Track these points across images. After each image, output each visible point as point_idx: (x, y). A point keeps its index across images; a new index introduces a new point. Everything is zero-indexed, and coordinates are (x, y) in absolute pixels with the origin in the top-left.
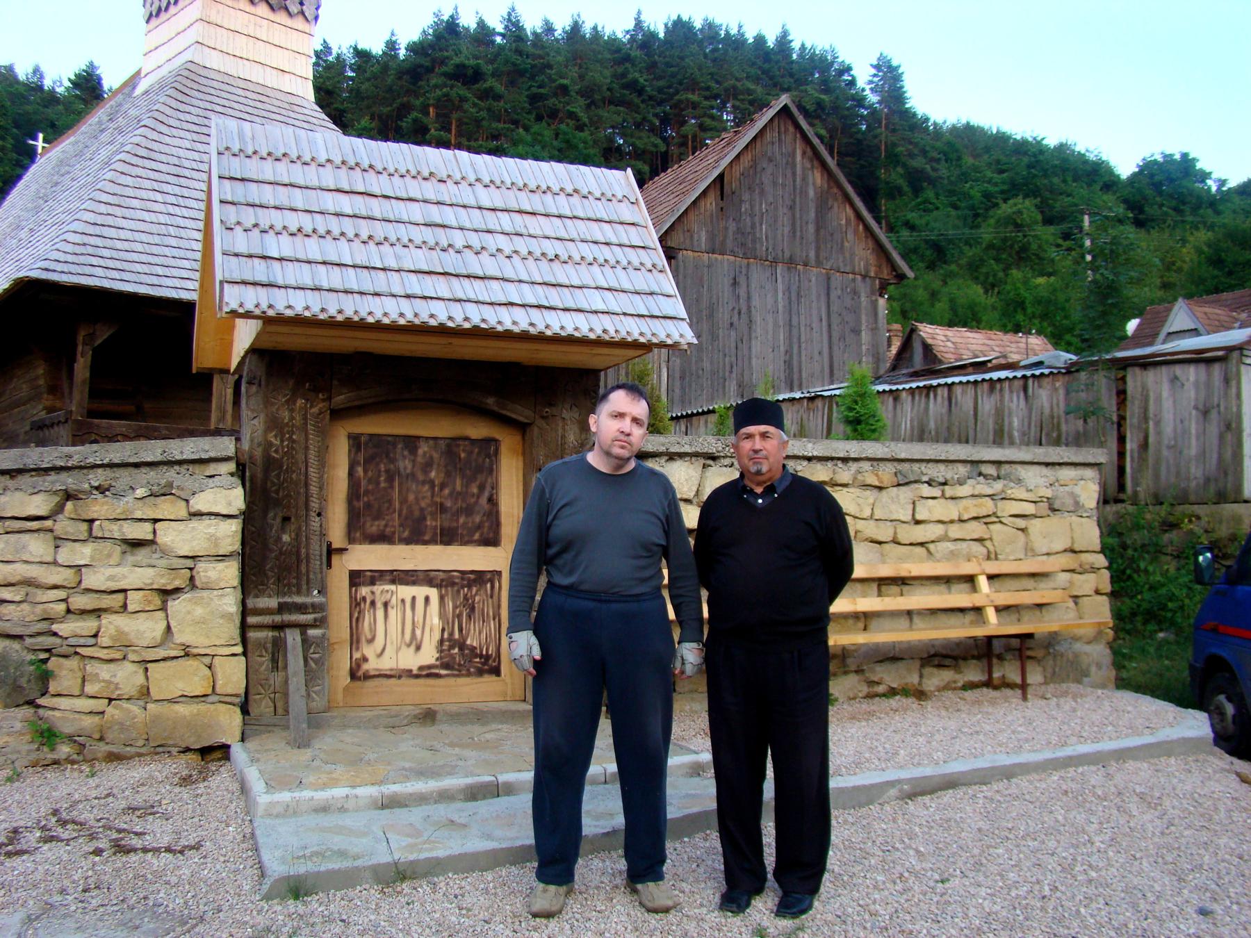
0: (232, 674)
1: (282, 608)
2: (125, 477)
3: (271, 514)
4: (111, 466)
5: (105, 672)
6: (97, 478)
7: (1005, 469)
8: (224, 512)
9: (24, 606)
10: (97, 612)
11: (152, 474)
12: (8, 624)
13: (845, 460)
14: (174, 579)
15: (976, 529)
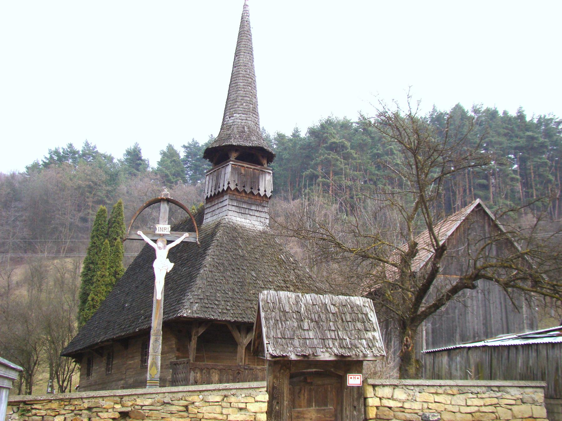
2: (239, 392)
4: (236, 389)
6: (233, 392)
7: (501, 389)
11: (246, 391)
13: (440, 386)
15: (491, 409)
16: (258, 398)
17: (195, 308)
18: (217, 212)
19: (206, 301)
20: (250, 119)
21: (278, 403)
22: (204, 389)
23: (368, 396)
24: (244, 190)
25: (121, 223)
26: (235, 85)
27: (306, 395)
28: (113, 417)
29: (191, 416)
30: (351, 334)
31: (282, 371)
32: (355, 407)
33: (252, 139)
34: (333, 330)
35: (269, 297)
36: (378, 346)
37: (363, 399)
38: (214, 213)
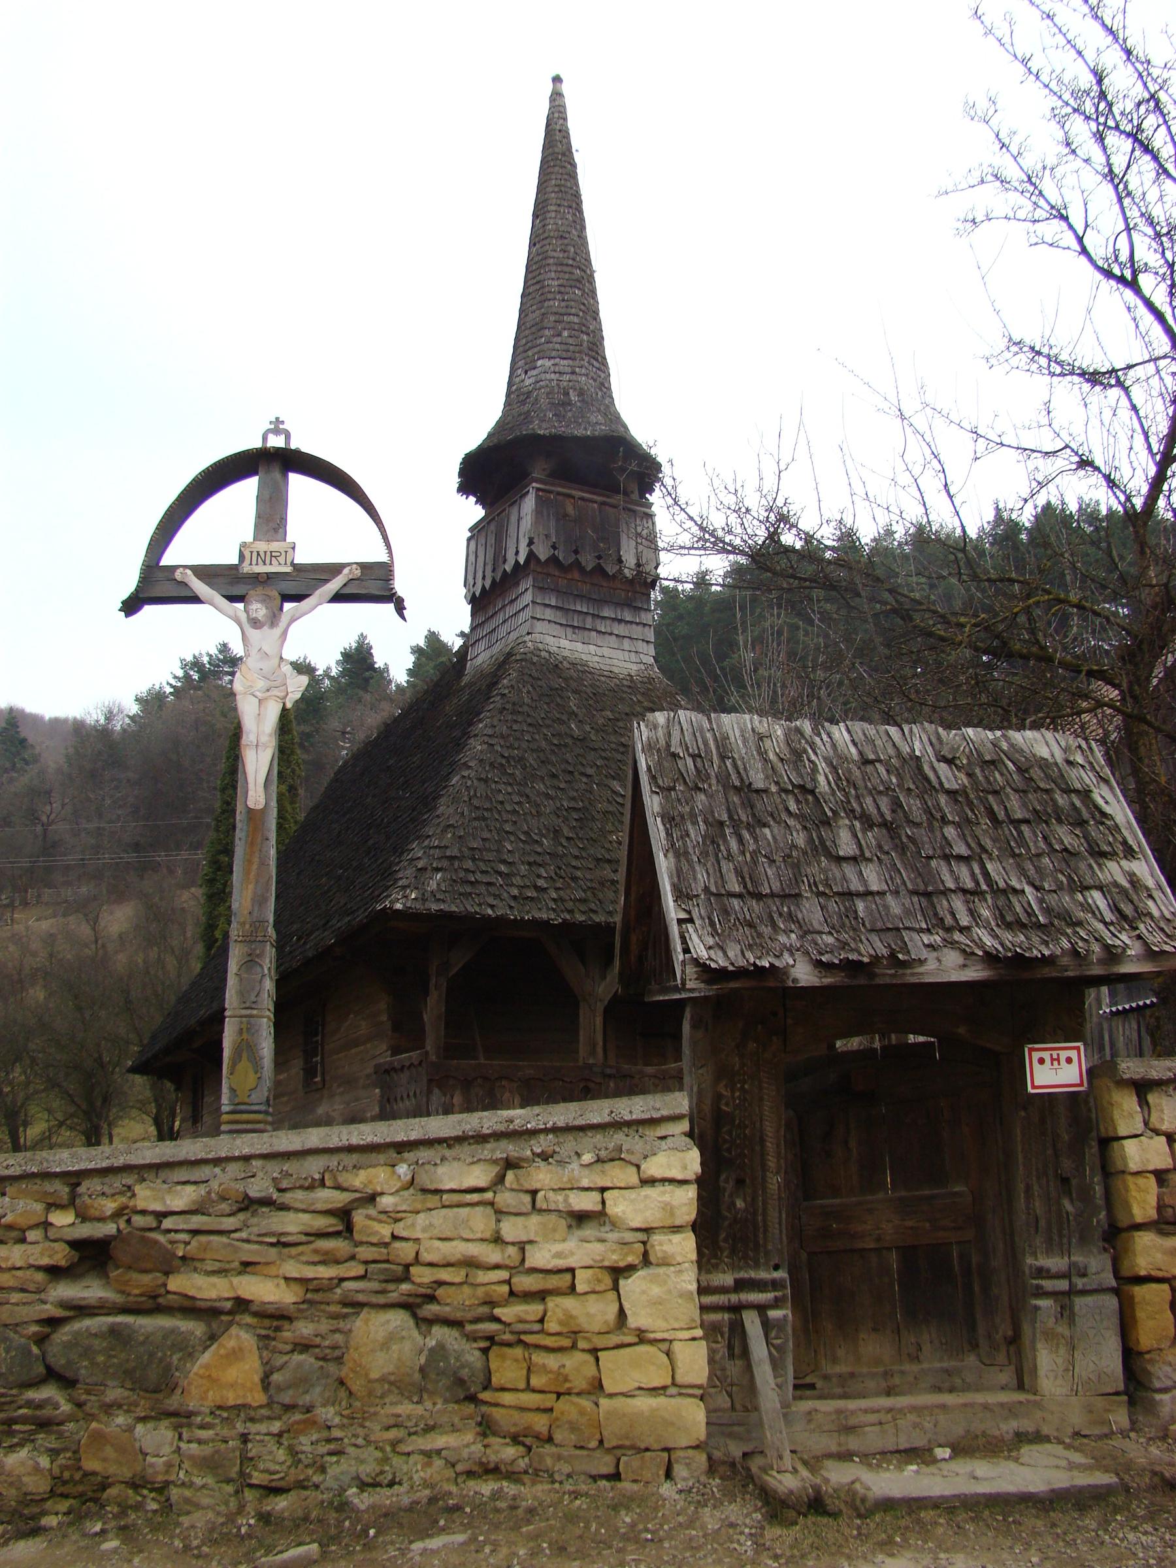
0: (694, 1361)
1: (741, 1285)
2: (569, 1144)
3: (723, 1177)
4: (555, 1130)
5: (552, 1361)
6: (543, 1143)
8: (680, 1177)
9: (466, 1290)
10: (541, 1296)
11: (598, 1138)
12: (447, 1309)
14: (627, 1254)
16: (653, 1168)
17: (433, 885)
18: (502, 631)
19: (469, 864)
20: (583, 371)
21: (740, 1182)
22: (413, 1136)
23: (1122, 1132)
24: (577, 563)
25: (288, 752)
26: (537, 287)
27: (853, 1143)
28: (45, 1261)
29: (365, 1253)
30: (1038, 870)
31: (752, 1046)
32: (1065, 1181)
33: (593, 419)
34: (960, 858)
35: (676, 734)
36: (1156, 913)
37: (1094, 1144)
38: (494, 637)
